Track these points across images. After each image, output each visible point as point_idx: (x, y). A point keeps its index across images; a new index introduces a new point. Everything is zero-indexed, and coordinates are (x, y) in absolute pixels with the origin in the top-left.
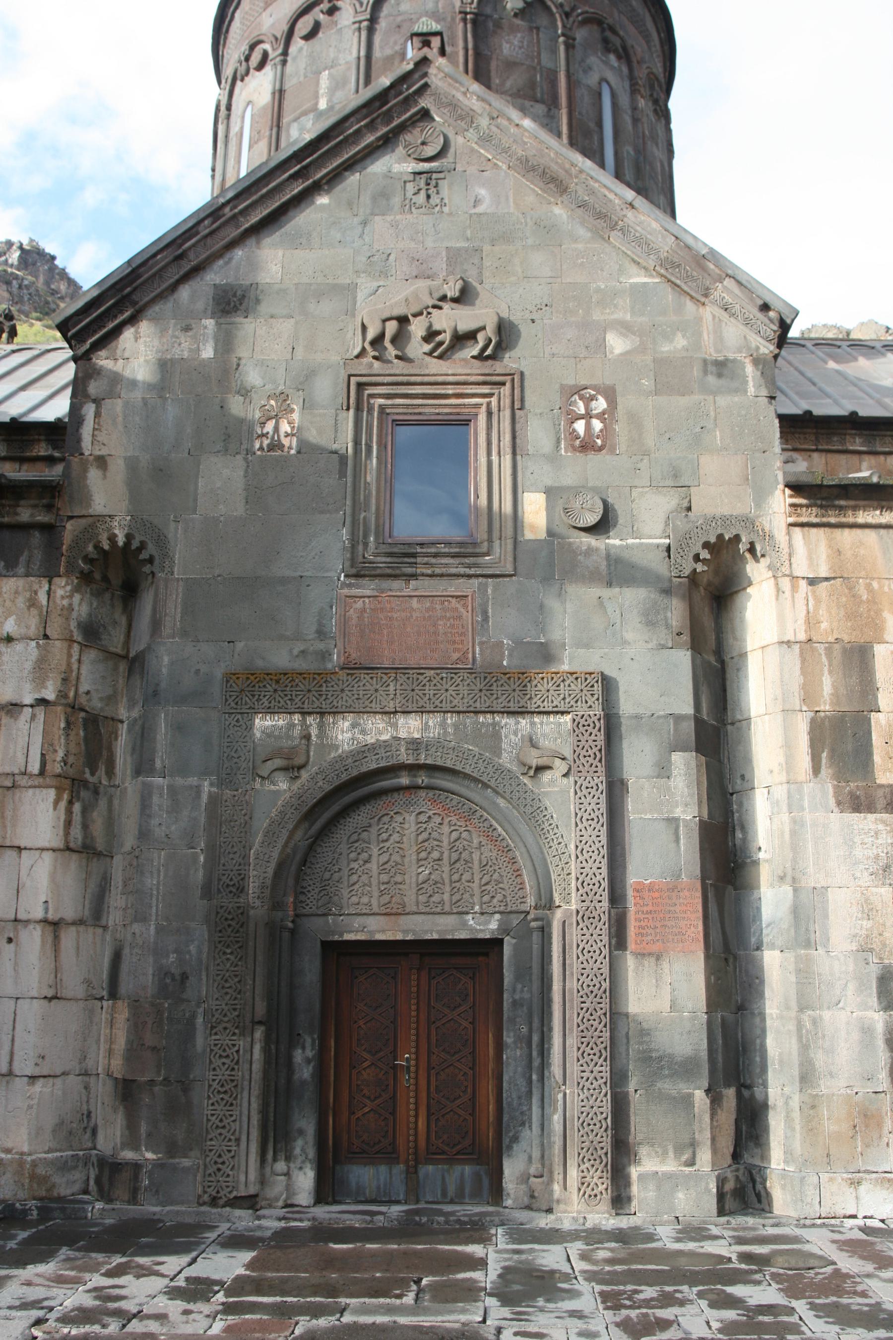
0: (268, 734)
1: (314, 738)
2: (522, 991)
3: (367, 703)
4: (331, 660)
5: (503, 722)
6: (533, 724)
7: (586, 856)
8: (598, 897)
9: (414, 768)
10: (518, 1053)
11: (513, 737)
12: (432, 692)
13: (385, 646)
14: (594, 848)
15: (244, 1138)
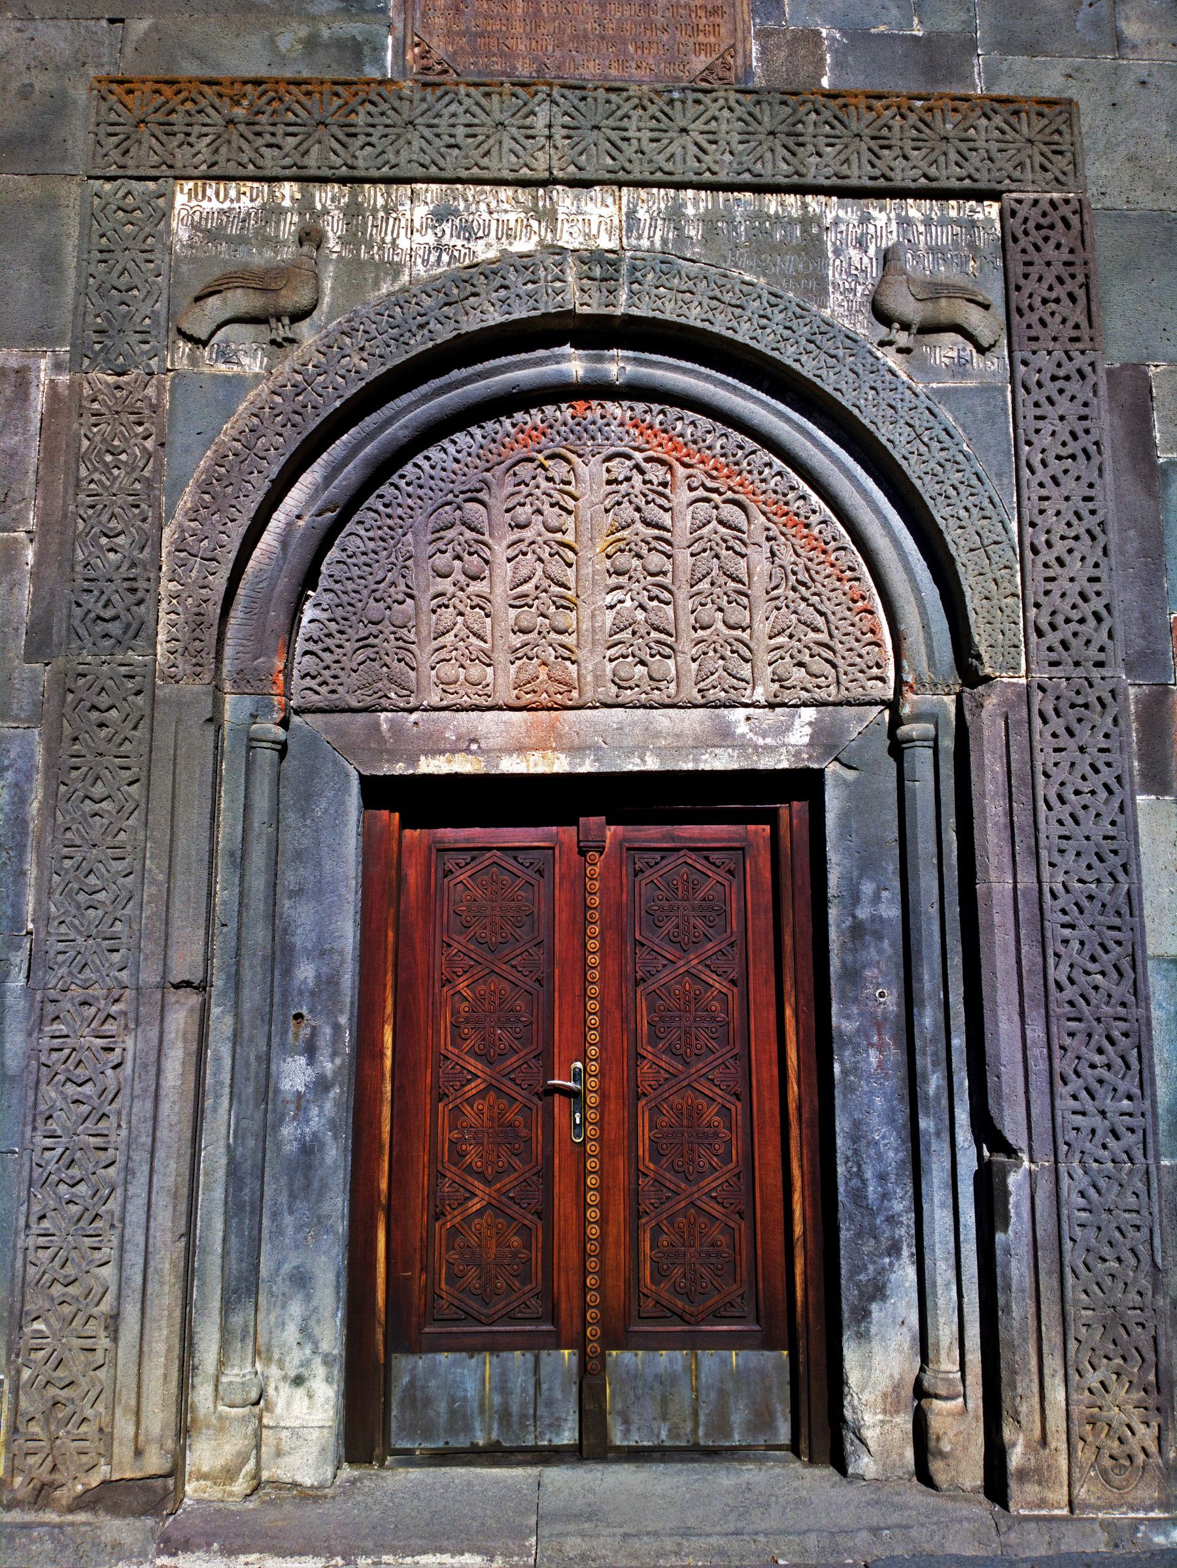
0: (209, 232)
1: (332, 243)
2: (876, 899)
3: (476, 154)
4: (379, 61)
5: (828, 219)
6: (905, 222)
7: (1060, 547)
8: (1093, 653)
9: (596, 333)
10: (873, 1057)
11: (855, 254)
12: (646, 135)
13: (519, 29)
14: (1079, 528)
15: (131, 1312)
